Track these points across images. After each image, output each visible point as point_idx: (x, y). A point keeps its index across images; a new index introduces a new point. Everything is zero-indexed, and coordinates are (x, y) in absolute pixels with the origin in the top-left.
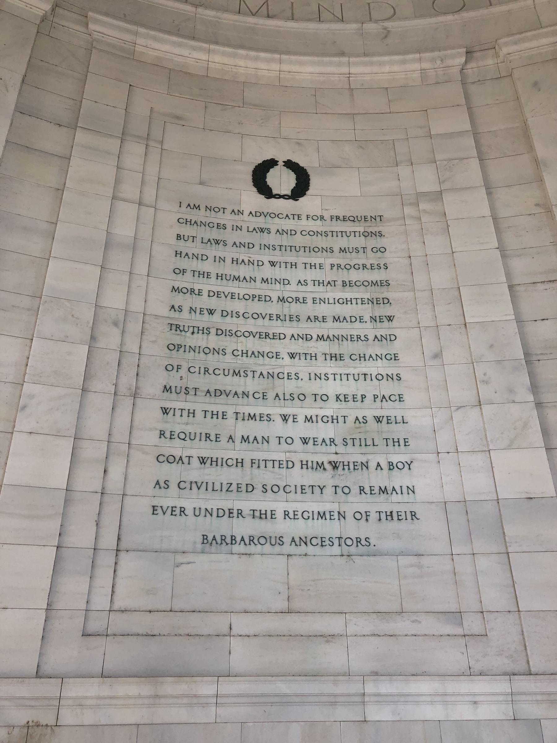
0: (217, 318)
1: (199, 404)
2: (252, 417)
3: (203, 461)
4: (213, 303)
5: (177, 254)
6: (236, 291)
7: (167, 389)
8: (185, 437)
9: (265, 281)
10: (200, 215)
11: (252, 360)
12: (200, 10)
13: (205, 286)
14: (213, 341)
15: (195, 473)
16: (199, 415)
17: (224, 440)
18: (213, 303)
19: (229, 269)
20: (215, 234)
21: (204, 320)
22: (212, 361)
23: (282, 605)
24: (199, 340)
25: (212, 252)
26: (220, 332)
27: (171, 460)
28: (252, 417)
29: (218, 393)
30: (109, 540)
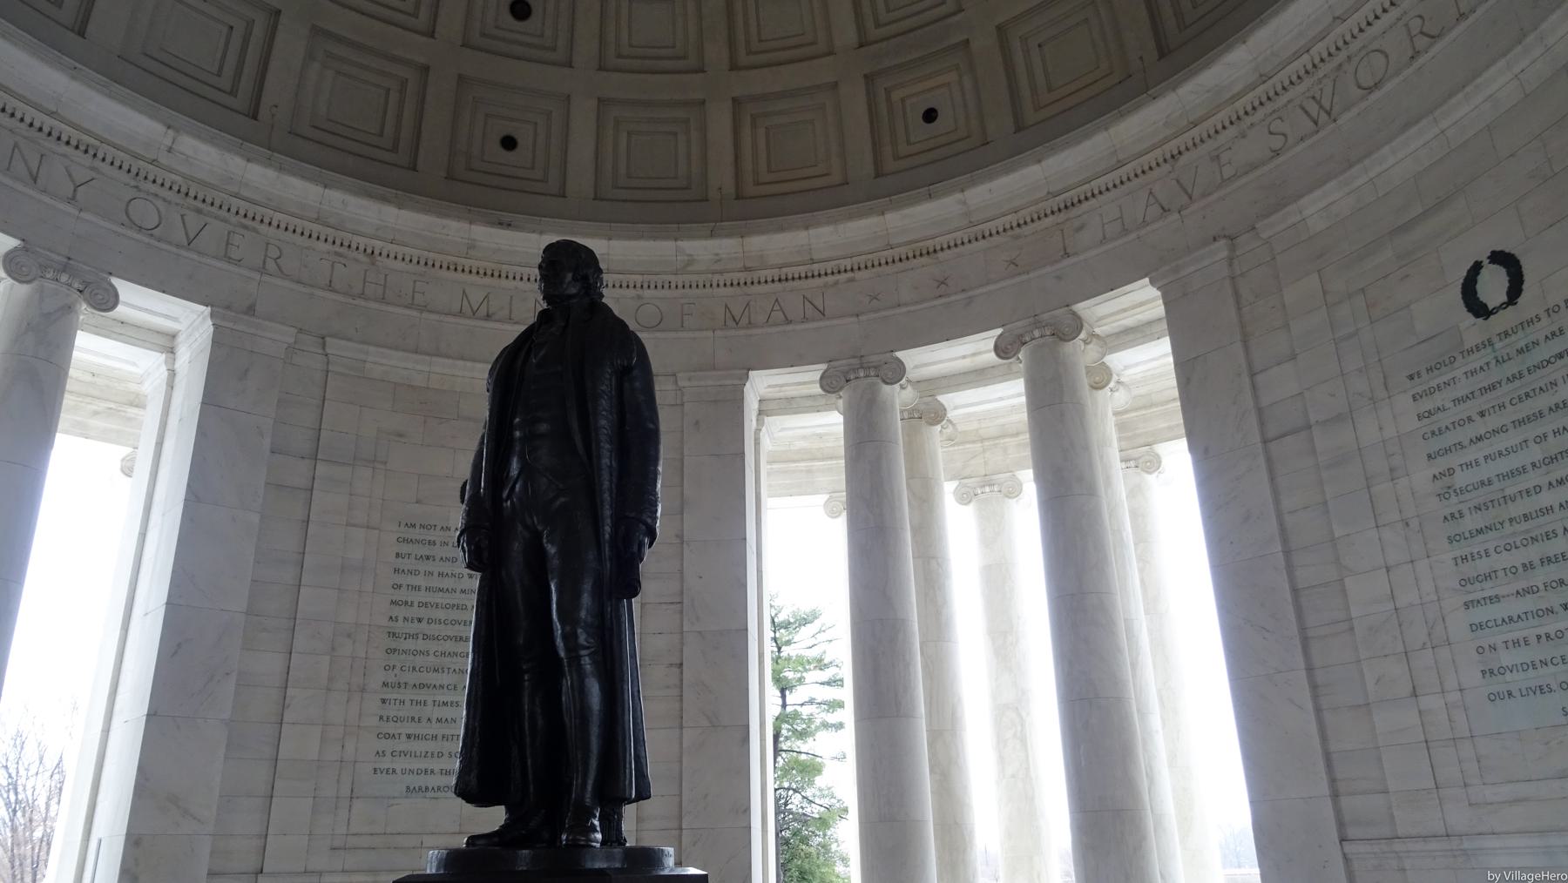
0: (424, 624)
1: (408, 695)
2: (445, 704)
3: (409, 737)
4: (422, 612)
5: (396, 571)
6: (439, 601)
7: (385, 684)
8: (397, 720)
9: (463, 591)
10: (415, 534)
11: (448, 659)
12: (425, 315)
13: (417, 597)
14: (420, 644)
15: (403, 745)
16: (408, 703)
17: (424, 721)
18: (422, 612)
19: (436, 582)
20: (425, 551)
21: (413, 628)
22: (419, 661)
23: (457, 829)
24: (410, 645)
25: (423, 567)
26: (426, 637)
27: (388, 736)
28: (445, 704)
29: (422, 686)
30: (346, 792)
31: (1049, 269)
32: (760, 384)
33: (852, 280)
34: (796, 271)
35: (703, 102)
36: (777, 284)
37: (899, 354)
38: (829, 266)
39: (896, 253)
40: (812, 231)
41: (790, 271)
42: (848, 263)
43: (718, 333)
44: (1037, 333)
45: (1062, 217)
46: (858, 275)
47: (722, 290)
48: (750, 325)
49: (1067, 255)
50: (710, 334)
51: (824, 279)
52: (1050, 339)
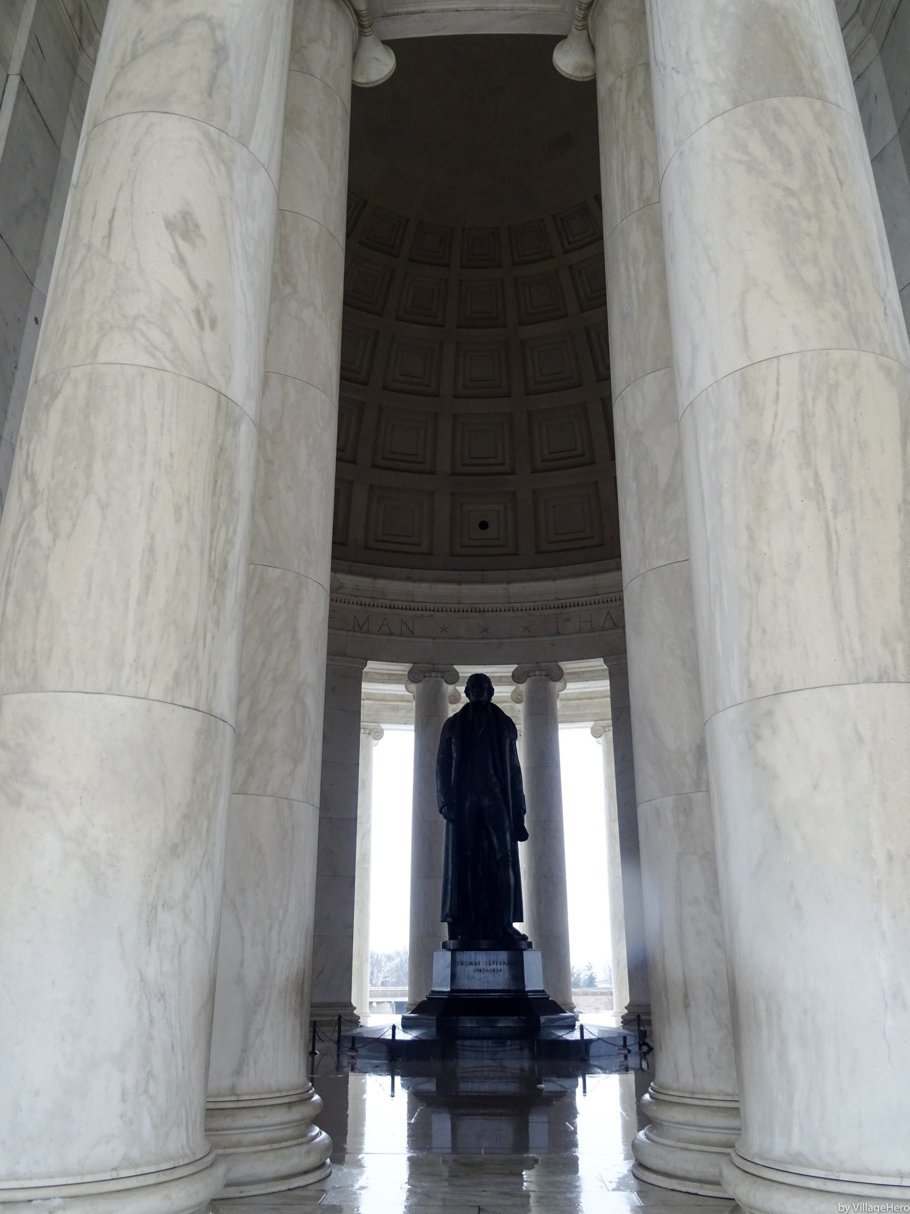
31: (548, 638)
32: (372, 666)
33: (432, 616)
34: (400, 604)
35: (352, 482)
36: (388, 610)
37: (455, 667)
38: (420, 606)
39: (461, 607)
40: (416, 584)
41: (397, 603)
42: (432, 606)
43: (350, 633)
44: (538, 673)
45: (558, 611)
46: (436, 614)
47: (354, 607)
48: (368, 632)
49: (558, 633)
50: (345, 633)
51: (416, 612)
52: (544, 678)
